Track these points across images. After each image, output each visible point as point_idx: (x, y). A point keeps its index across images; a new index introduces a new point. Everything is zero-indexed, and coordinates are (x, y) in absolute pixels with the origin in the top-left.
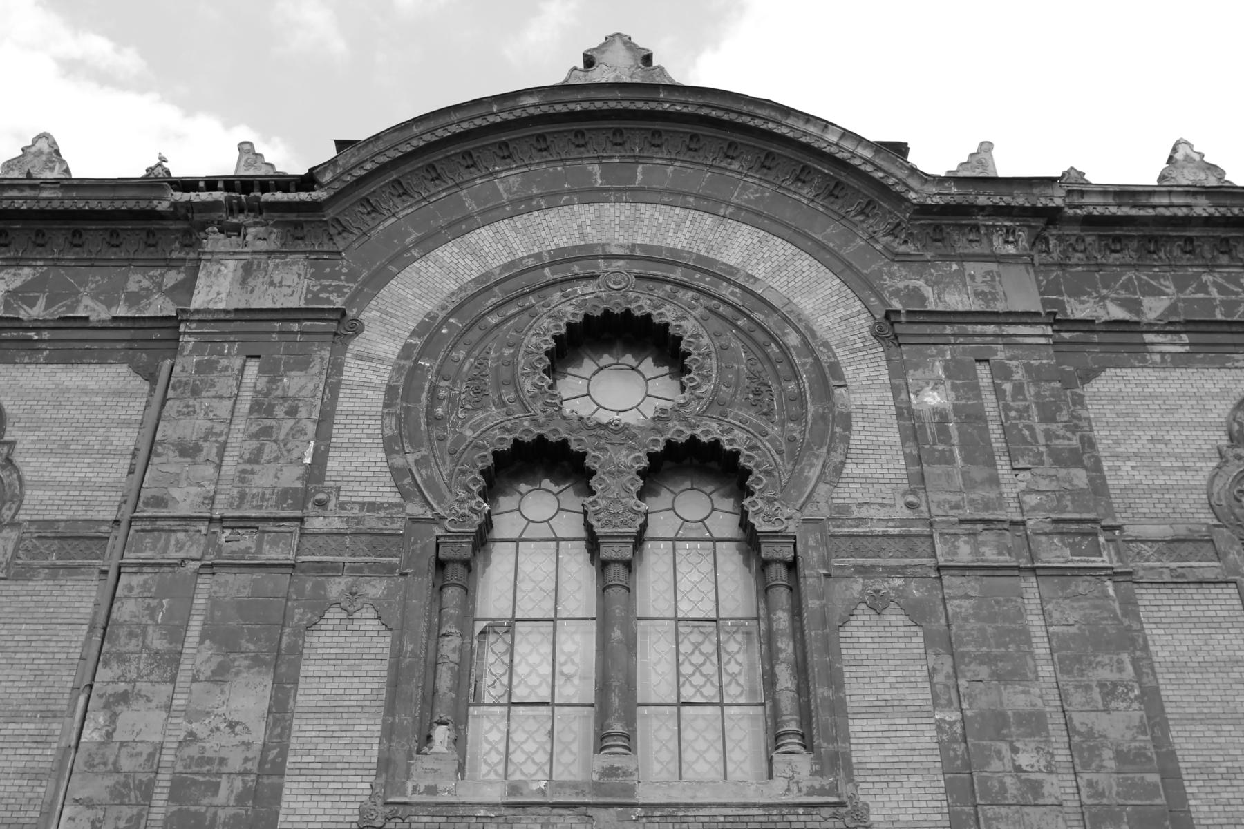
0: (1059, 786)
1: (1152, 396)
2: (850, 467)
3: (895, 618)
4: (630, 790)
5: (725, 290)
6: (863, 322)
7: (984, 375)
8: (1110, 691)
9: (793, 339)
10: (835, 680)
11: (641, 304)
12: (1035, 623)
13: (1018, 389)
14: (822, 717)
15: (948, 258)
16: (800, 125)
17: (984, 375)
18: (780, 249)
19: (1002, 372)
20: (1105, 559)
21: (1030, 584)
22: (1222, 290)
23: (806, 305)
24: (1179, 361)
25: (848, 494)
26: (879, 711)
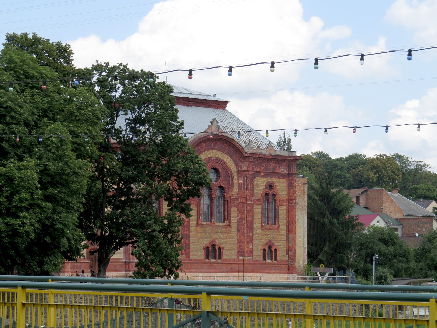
0: (245, 225)
1: (260, 181)
2: (233, 190)
3: (235, 207)
4: (215, 224)
5: (224, 165)
6: (236, 170)
7: (246, 177)
8: (250, 216)
9: (230, 173)
10: (230, 214)
11: (216, 167)
12: (246, 208)
13: (249, 180)
14: (229, 217)
15: (245, 161)
16: (235, 143)
17: (246, 177)
18: (230, 158)
19: (247, 178)
20: (252, 202)
21: (246, 204)
22: (269, 166)
23: (232, 167)
24: (263, 177)
25: (233, 193)
26: (233, 217)
